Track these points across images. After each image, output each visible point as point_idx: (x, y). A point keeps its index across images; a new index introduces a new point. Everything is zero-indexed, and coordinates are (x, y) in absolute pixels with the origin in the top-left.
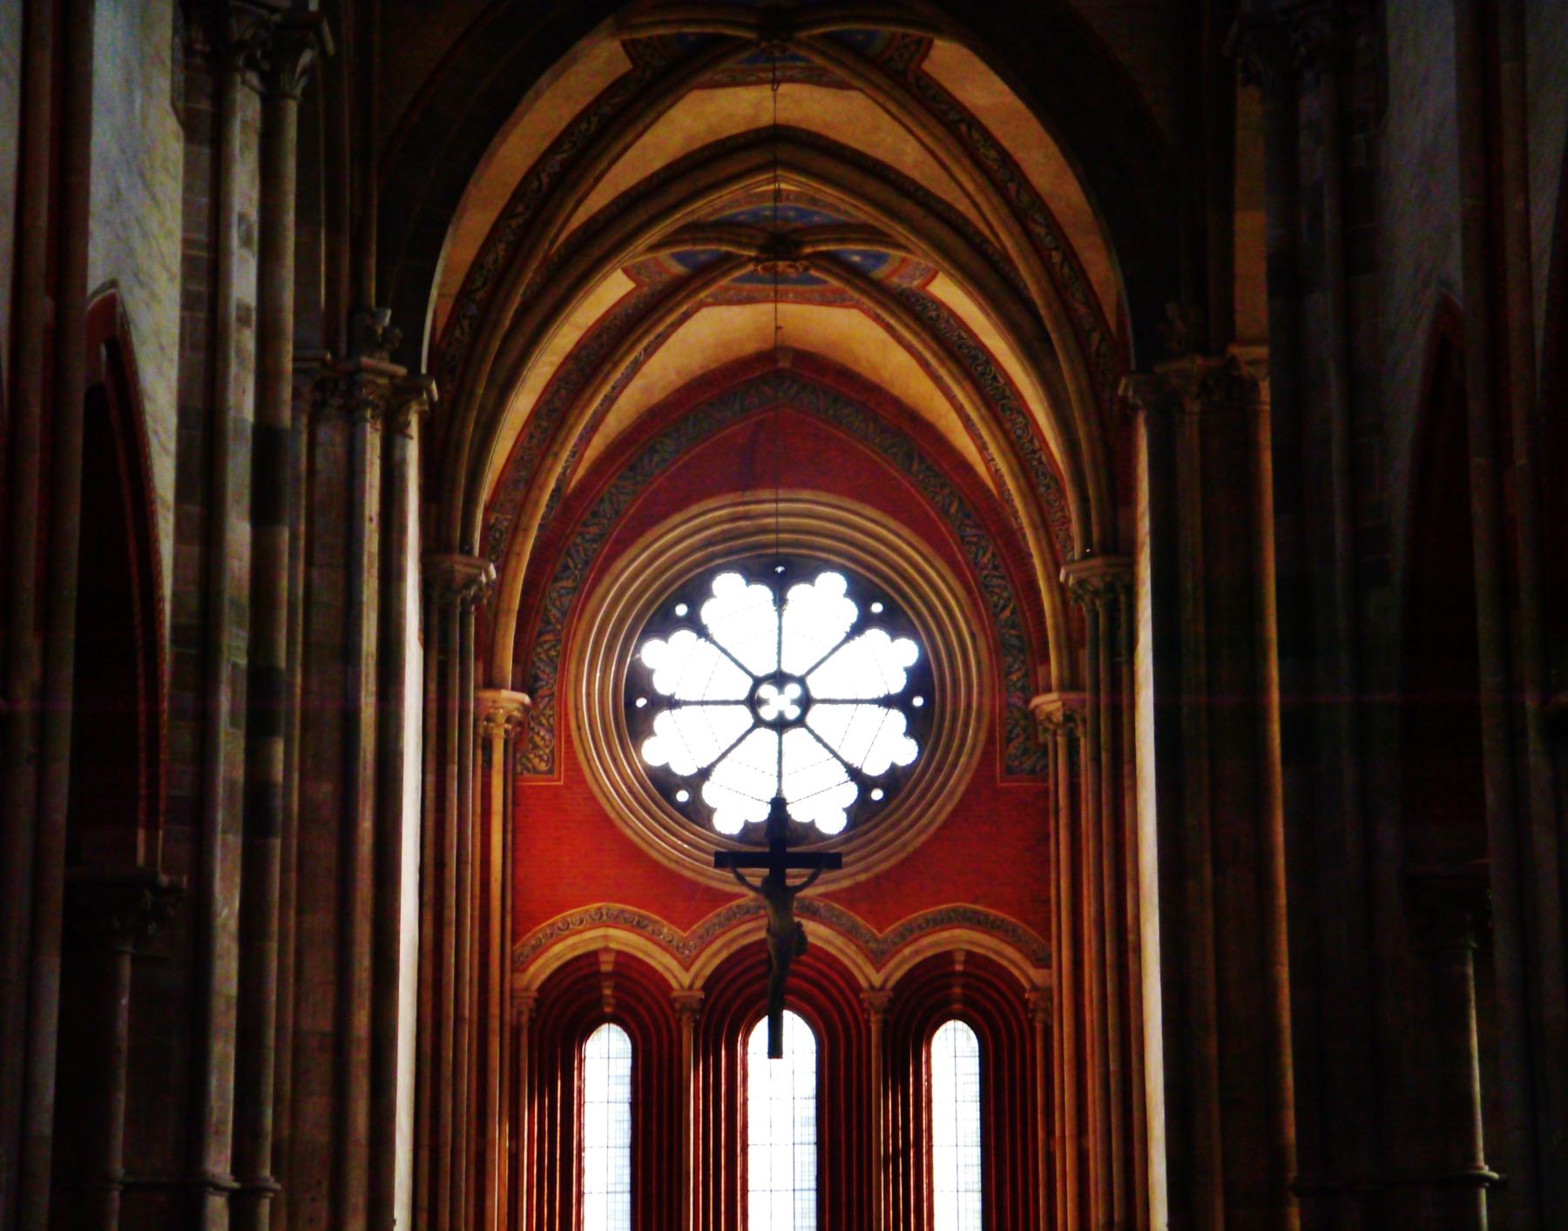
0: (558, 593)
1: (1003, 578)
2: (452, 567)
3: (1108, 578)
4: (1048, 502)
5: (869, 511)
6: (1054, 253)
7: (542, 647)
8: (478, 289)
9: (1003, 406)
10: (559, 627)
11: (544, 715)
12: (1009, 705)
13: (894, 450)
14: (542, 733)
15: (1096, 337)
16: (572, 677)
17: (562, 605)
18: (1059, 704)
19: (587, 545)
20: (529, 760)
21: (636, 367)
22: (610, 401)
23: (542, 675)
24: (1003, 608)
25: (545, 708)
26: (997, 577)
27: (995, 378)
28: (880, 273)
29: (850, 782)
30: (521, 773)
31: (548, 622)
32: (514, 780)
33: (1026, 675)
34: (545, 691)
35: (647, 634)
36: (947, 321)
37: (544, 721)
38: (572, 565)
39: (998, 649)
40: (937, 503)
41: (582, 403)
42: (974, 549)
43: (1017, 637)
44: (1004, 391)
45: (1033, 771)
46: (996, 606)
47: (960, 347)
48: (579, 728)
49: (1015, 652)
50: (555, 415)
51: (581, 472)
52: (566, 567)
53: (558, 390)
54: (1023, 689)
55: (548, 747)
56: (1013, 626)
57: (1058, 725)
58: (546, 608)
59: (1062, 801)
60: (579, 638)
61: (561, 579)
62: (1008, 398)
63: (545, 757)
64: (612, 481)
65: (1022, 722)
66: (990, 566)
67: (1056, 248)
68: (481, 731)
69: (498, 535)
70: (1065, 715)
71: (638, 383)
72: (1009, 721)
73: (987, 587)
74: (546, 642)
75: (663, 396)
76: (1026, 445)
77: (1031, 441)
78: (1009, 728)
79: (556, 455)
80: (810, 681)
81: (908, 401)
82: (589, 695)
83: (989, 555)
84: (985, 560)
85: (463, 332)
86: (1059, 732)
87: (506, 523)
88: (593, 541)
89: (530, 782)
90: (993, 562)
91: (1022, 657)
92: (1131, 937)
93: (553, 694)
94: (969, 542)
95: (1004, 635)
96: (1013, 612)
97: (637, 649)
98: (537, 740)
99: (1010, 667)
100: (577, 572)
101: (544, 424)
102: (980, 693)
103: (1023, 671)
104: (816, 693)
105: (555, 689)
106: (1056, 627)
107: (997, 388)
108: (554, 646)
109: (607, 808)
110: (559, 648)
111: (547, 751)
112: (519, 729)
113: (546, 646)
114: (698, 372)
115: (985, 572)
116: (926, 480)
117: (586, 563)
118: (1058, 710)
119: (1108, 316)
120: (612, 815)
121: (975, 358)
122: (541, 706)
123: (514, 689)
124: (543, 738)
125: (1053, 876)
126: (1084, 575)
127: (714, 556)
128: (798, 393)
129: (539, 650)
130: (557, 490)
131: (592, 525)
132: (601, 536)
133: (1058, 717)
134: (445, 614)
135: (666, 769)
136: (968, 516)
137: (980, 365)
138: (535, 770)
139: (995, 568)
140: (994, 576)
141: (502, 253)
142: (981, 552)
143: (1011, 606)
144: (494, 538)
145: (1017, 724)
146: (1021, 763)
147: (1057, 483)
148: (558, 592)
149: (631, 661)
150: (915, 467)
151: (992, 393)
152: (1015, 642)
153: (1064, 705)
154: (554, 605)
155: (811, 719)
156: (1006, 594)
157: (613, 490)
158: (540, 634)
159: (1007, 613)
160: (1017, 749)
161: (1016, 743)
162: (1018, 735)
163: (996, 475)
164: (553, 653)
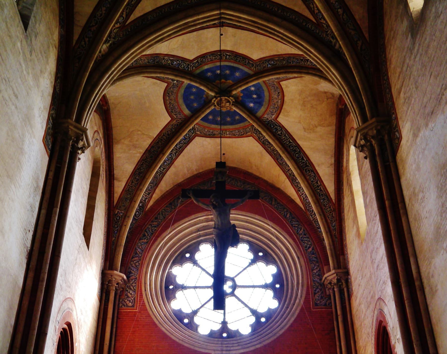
0: (140, 245)
1: (308, 238)
2: (68, 126)
3: (379, 127)
4: (324, 205)
5: (257, 217)
6: (339, 10)
7: (133, 262)
8: (93, 26)
9: (306, 170)
10: (140, 255)
11: (132, 286)
12: (314, 281)
13: (266, 198)
14: (131, 292)
15: (360, 43)
16: (144, 270)
17: (142, 248)
18: (335, 275)
19: (152, 228)
20: (125, 301)
21: (171, 161)
22: (162, 174)
23: (132, 272)
24: (309, 248)
25: (133, 283)
26: (306, 238)
27: (303, 159)
28: (260, 113)
29: (252, 316)
30: (122, 307)
31: (136, 253)
32: (118, 309)
33: (320, 270)
34: (133, 277)
35: (174, 263)
36: (285, 136)
37: (132, 288)
38: (147, 235)
39: (309, 261)
40: (282, 214)
41: (151, 170)
42: (296, 228)
43: (315, 258)
44: (306, 163)
45: (325, 305)
46: (306, 247)
47: (289, 146)
48: (148, 302)
49: (315, 263)
50: (141, 175)
51: (151, 203)
52: (145, 235)
53: (142, 164)
54: (319, 275)
55: (133, 297)
56: (313, 254)
57: (335, 284)
58: (136, 249)
59: (339, 312)
60: (148, 259)
61: (142, 239)
62: (308, 166)
63: (131, 301)
64: (163, 208)
65: (320, 287)
66: (303, 234)
67: (340, 8)
68: (106, 287)
69: (118, 218)
70: (337, 279)
71: (172, 170)
72: (314, 287)
73: (302, 241)
74: (135, 260)
75: (182, 180)
76: (315, 184)
77: (317, 183)
78: (314, 289)
79: (141, 190)
80: (236, 279)
81: (270, 181)
82: (150, 281)
83: (302, 230)
84: (301, 232)
85: (85, 44)
86: (335, 287)
87: (121, 214)
88: (155, 227)
89: (124, 310)
90: (304, 233)
91: (317, 264)
92: (417, 283)
93: (136, 278)
94: (294, 226)
95: (310, 257)
96: (313, 249)
97: (171, 268)
98: (129, 294)
99: (313, 268)
100: (148, 237)
101: (137, 177)
102: (302, 278)
103: (318, 269)
104: (238, 283)
105: (137, 276)
106: (331, 250)
107: (304, 163)
108: (138, 262)
109: (155, 320)
110: (139, 262)
111: (132, 299)
112: (121, 289)
113: (135, 262)
114: (195, 173)
115: (301, 236)
116: (278, 207)
117: (152, 234)
118: (334, 278)
119: (364, 33)
120: (157, 322)
121: (295, 151)
122: (131, 283)
123: (120, 272)
124: (131, 294)
125: (338, 343)
126: (365, 131)
127: (200, 236)
128: (231, 181)
129: (132, 263)
130: (142, 207)
131: (155, 222)
132: (158, 225)
133: (335, 281)
134: (63, 149)
135: (180, 311)
136: (293, 218)
137: (297, 154)
138: (127, 306)
139: (305, 235)
140: (305, 237)
141: (104, 12)
142: (299, 229)
143: (312, 247)
144: (117, 219)
145: (317, 288)
146: (321, 302)
147: (327, 197)
148: (141, 243)
149: (168, 272)
150: (273, 203)
151: (302, 165)
152: (315, 259)
153: (337, 275)
154: (139, 248)
155: (236, 292)
156: (310, 243)
157: (163, 211)
158: (133, 257)
159: (311, 249)
160: (318, 297)
161: (317, 295)
162: (318, 292)
163: (304, 201)
164: (137, 264)
